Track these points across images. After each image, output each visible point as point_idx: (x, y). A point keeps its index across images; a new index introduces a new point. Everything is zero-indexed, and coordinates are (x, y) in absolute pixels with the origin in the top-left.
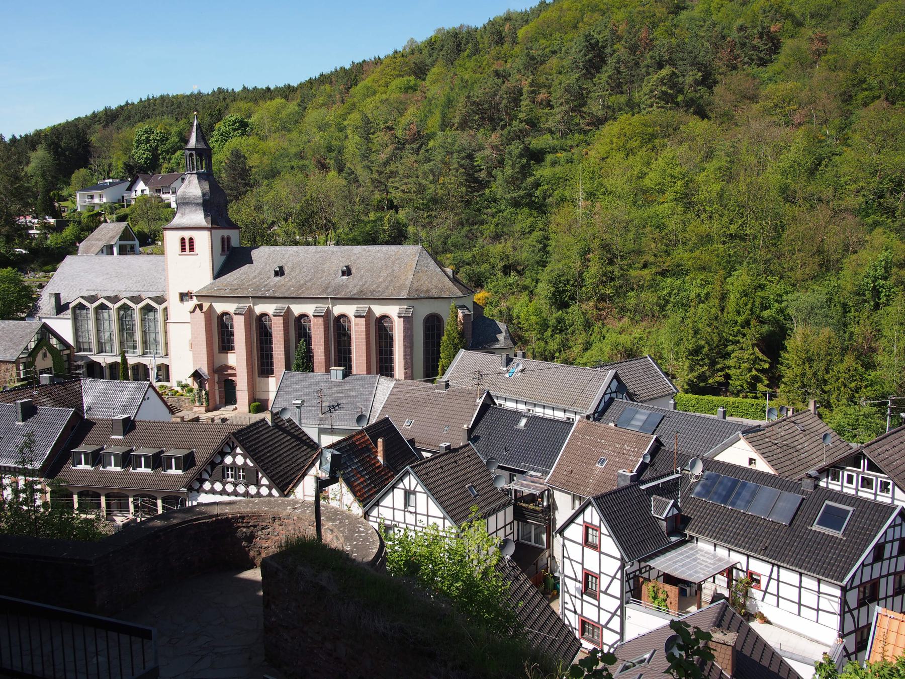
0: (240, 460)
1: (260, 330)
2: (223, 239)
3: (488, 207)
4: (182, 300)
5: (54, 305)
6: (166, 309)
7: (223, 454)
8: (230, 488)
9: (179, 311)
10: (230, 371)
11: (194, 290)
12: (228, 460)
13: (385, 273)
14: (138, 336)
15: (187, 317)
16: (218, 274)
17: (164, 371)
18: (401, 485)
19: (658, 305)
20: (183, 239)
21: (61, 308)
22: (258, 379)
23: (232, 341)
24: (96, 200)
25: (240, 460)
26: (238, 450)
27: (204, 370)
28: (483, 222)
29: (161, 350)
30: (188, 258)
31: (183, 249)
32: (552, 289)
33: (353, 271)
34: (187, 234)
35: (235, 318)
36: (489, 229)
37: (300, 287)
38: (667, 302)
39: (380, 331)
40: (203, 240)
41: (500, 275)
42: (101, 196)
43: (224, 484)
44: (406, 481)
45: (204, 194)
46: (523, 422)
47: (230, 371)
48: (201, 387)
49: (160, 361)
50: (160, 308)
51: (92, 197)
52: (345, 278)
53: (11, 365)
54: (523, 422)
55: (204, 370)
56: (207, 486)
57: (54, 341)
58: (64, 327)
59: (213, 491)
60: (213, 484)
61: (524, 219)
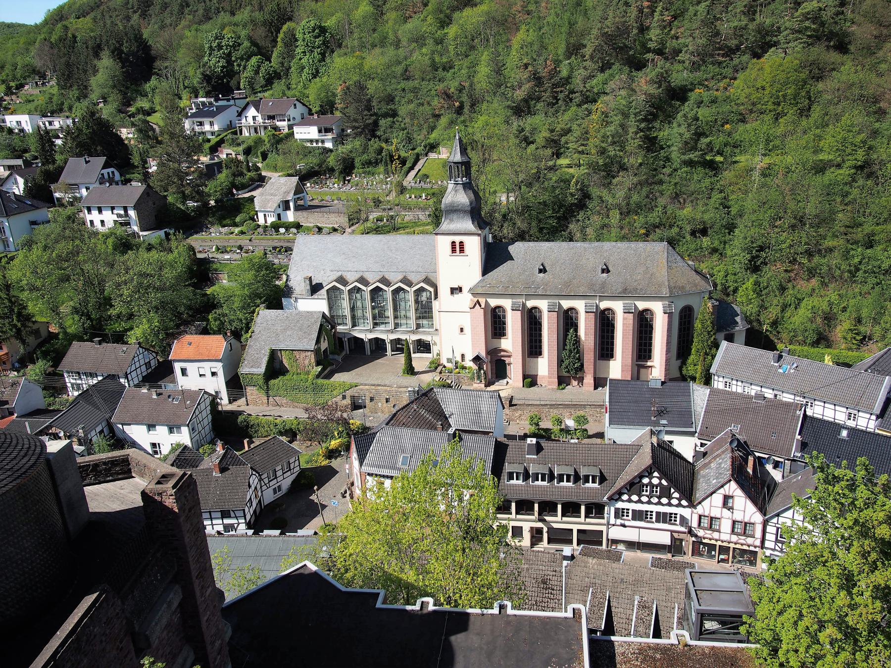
1: (532, 321)
3: (664, 167)
4: (452, 293)
5: (308, 287)
8: (645, 499)
10: (502, 353)
12: (646, 481)
13: (641, 270)
14: (390, 313)
16: (486, 270)
19: (850, 271)
20: (453, 243)
22: (528, 359)
23: (504, 329)
24: (207, 128)
25: (655, 481)
26: (656, 474)
27: (483, 354)
28: (661, 182)
30: (458, 259)
31: (454, 250)
32: (748, 256)
33: (610, 268)
34: (457, 239)
36: (668, 189)
37: (567, 284)
38: (858, 270)
39: (643, 325)
41: (688, 237)
42: (212, 124)
43: (640, 496)
45: (471, 203)
47: (502, 353)
48: (480, 368)
51: (201, 124)
52: (605, 275)
53: (309, 353)
55: (483, 354)
56: (625, 497)
59: (630, 501)
60: (630, 496)
61: (700, 179)
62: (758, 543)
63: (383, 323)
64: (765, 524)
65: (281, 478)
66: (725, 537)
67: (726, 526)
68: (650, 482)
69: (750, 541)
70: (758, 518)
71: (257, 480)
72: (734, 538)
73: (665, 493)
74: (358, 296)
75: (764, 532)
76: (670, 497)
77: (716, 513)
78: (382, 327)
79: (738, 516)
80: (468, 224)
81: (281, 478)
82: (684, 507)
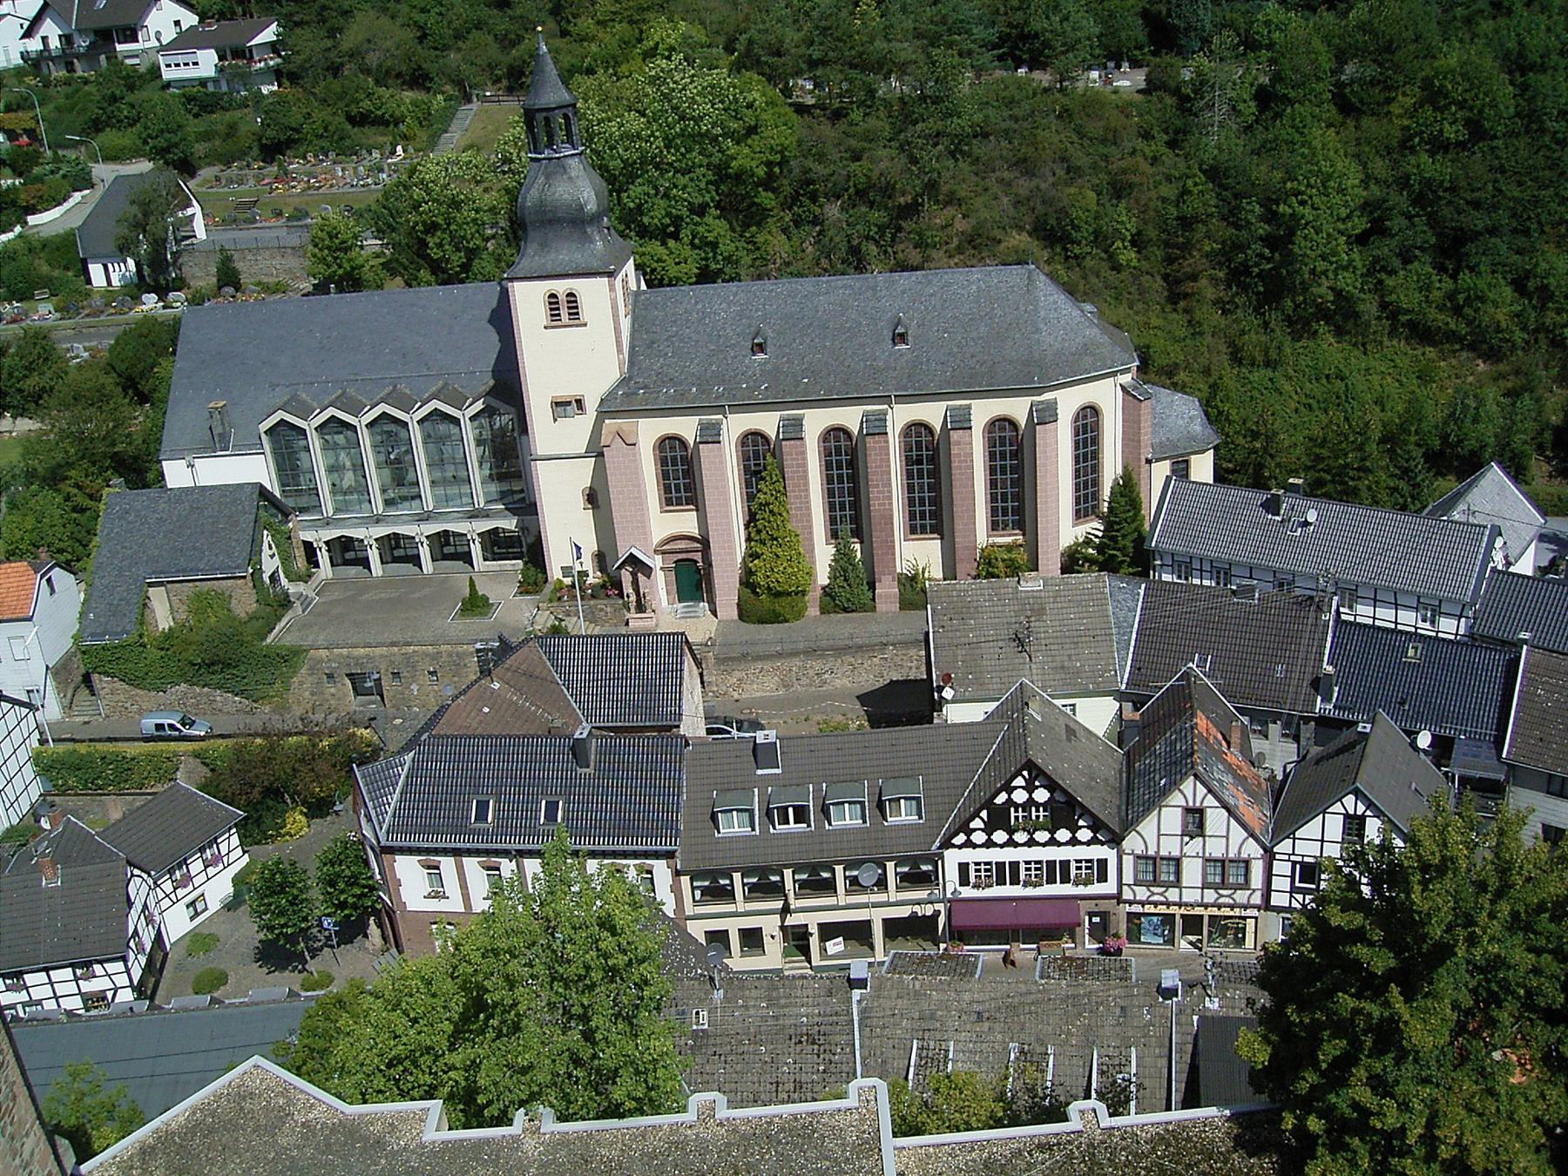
18: (1337, 807)
43: (1011, 832)
62: (1257, 899)
63: (404, 499)
64: (1270, 856)
65: (203, 877)
66: (1190, 896)
67: (1192, 872)
68: (1010, 800)
69: (1241, 896)
70: (1253, 850)
71: (145, 888)
72: (1210, 896)
75: (1269, 875)
77: (1170, 847)
78: (404, 510)
79: (1216, 849)
81: (203, 877)
82: (1102, 844)
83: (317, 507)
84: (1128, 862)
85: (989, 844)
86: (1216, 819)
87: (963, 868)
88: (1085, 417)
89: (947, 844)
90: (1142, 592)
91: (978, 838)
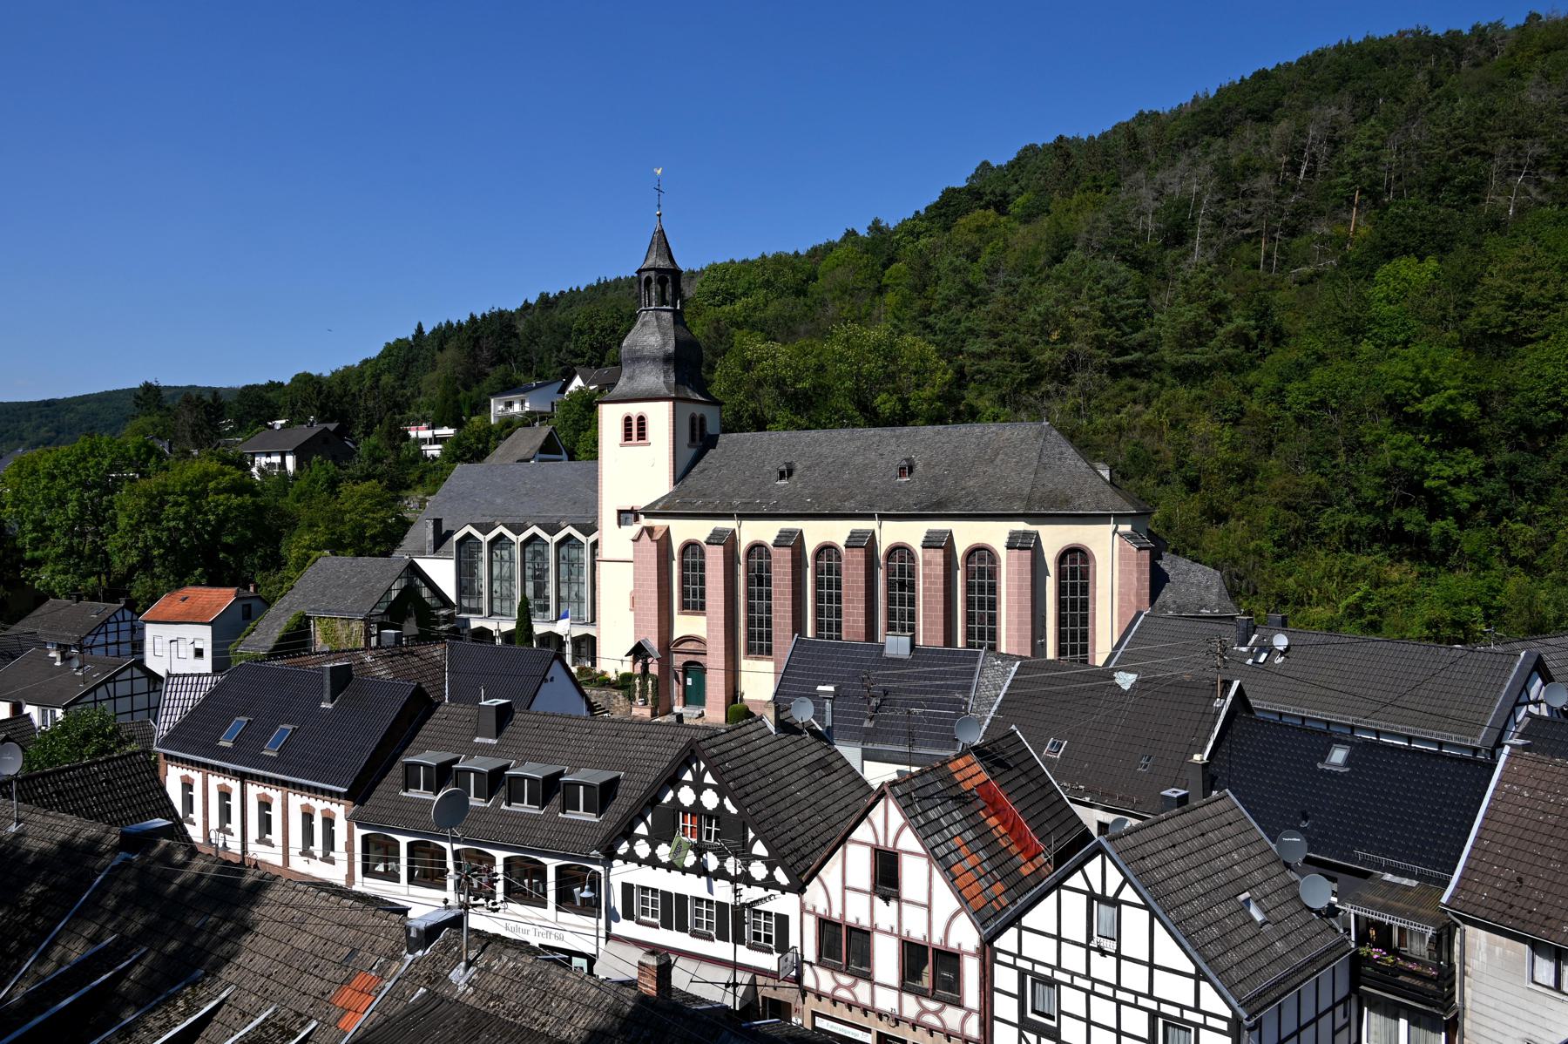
0: (710, 800)
2: (693, 419)
6: (595, 545)
7: (675, 782)
9: (615, 540)
11: (641, 502)
12: (687, 796)
15: (628, 551)
17: (587, 646)
18: (1076, 880)
20: (628, 420)
21: (441, 539)
24: (517, 408)
25: (710, 800)
29: (587, 615)
30: (635, 451)
31: (628, 436)
35: (709, 550)
40: (659, 416)
42: (522, 403)
44: (1093, 867)
45: (665, 344)
46: (1338, 756)
49: (578, 631)
50: (587, 541)
51: (510, 404)
54: (1338, 756)
57: (425, 593)
58: (442, 572)
64: (987, 954)
66: (887, 1000)
67: (886, 959)
69: (952, 1017)
70: (965, 936)
72: (911, 1007)
73: (729, 835)
74: (505, 553)
76: (747, 858)
77: (858, 911)
80: (653, 378)
83: (480, 612)
84: (811, 924)
85: (653, 861)
86: (915, 872)
87: (627, 889)
88: (1074, 561)
89: (610, 856)
90: (1014, 669)
91: (642, 849)
